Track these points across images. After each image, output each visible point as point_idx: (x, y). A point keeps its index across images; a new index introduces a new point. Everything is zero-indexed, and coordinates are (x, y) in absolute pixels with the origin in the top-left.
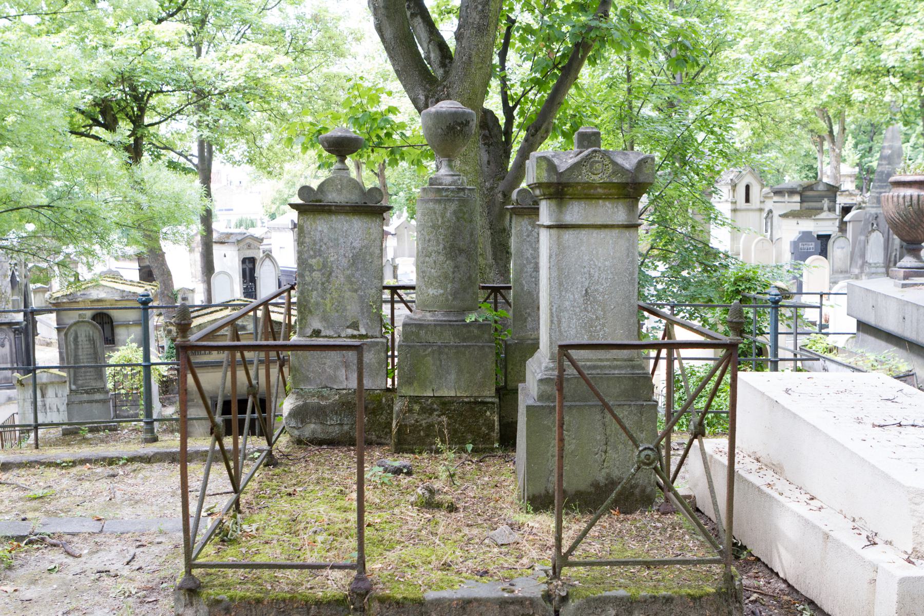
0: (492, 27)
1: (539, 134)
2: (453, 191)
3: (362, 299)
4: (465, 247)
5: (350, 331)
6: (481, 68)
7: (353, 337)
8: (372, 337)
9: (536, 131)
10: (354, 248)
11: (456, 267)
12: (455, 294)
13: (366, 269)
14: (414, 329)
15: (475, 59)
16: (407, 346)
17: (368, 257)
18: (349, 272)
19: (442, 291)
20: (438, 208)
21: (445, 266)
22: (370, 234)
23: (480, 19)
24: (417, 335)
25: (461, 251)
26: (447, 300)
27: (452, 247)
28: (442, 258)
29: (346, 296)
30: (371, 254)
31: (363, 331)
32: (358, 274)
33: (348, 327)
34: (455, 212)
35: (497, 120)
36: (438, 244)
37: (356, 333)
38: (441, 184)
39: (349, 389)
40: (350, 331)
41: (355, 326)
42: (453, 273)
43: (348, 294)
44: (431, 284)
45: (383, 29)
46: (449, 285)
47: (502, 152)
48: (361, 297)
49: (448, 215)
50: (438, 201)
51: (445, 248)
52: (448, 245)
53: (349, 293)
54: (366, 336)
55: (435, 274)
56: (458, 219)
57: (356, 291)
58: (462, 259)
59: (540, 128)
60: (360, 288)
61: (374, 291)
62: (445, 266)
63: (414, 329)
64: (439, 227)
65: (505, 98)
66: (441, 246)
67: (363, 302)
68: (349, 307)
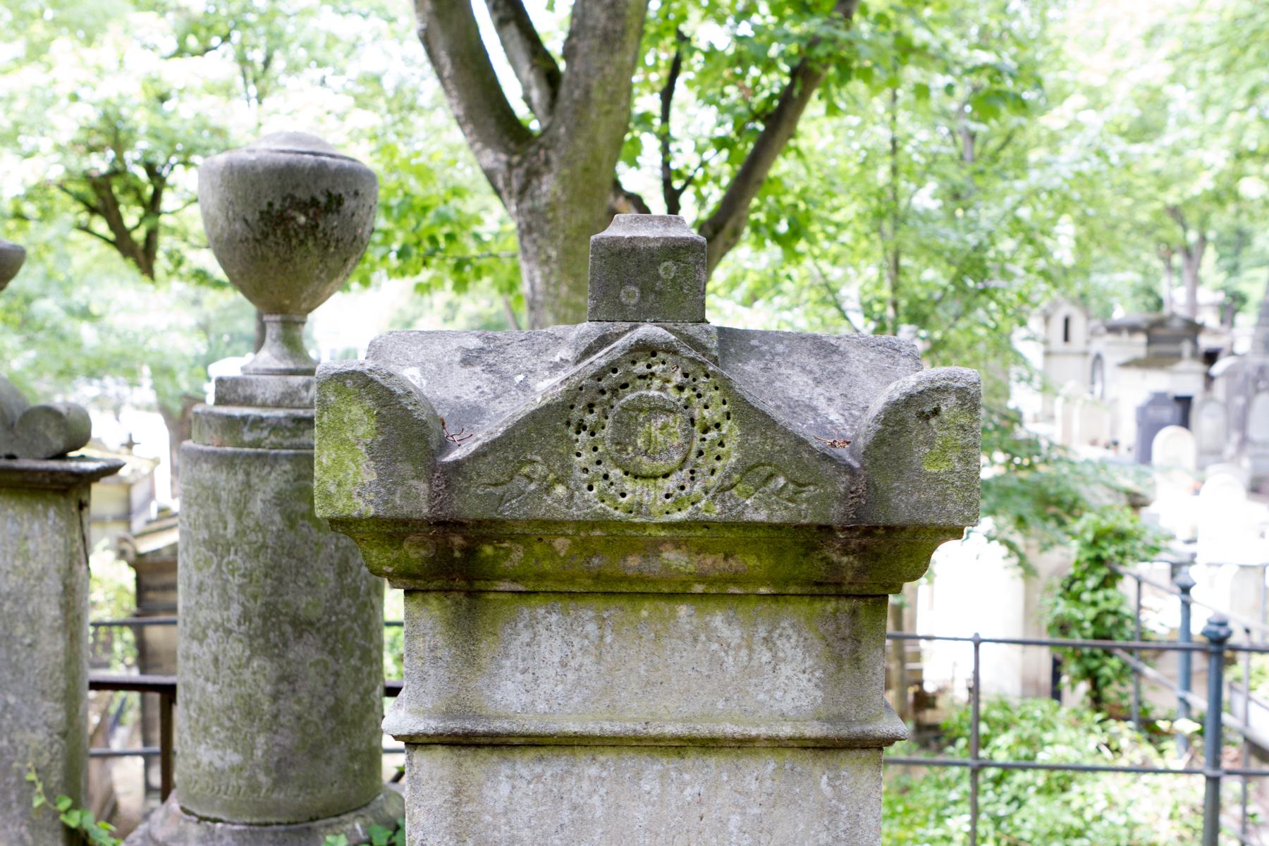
2: (276, 427)
4: (314, 614)
11: (283, 678)
12: (280, 769)
17: (20, 629)
19: (234, 758)
20: (227, 482)
21: (247, 675)
22: (27, 557)
25: (302, 626)
26: (254, 787)
27: (270, 613)
28: (237, 649)
30: (31, 621)
34: (280, 500)
36: (226, 601)
38: (248, 401)
42: (275, 697)
44: (206, 729)
46: (261, 740)
49: (257, 506)
50: (227, 461)
51: (246, 617)
52: (256, 607)
55: (217, 701)
56: (291, 521)
58: (306, 652)
61: (40, 735)
62: (247, 675)
64: (228, 546)
66: (236, 610)
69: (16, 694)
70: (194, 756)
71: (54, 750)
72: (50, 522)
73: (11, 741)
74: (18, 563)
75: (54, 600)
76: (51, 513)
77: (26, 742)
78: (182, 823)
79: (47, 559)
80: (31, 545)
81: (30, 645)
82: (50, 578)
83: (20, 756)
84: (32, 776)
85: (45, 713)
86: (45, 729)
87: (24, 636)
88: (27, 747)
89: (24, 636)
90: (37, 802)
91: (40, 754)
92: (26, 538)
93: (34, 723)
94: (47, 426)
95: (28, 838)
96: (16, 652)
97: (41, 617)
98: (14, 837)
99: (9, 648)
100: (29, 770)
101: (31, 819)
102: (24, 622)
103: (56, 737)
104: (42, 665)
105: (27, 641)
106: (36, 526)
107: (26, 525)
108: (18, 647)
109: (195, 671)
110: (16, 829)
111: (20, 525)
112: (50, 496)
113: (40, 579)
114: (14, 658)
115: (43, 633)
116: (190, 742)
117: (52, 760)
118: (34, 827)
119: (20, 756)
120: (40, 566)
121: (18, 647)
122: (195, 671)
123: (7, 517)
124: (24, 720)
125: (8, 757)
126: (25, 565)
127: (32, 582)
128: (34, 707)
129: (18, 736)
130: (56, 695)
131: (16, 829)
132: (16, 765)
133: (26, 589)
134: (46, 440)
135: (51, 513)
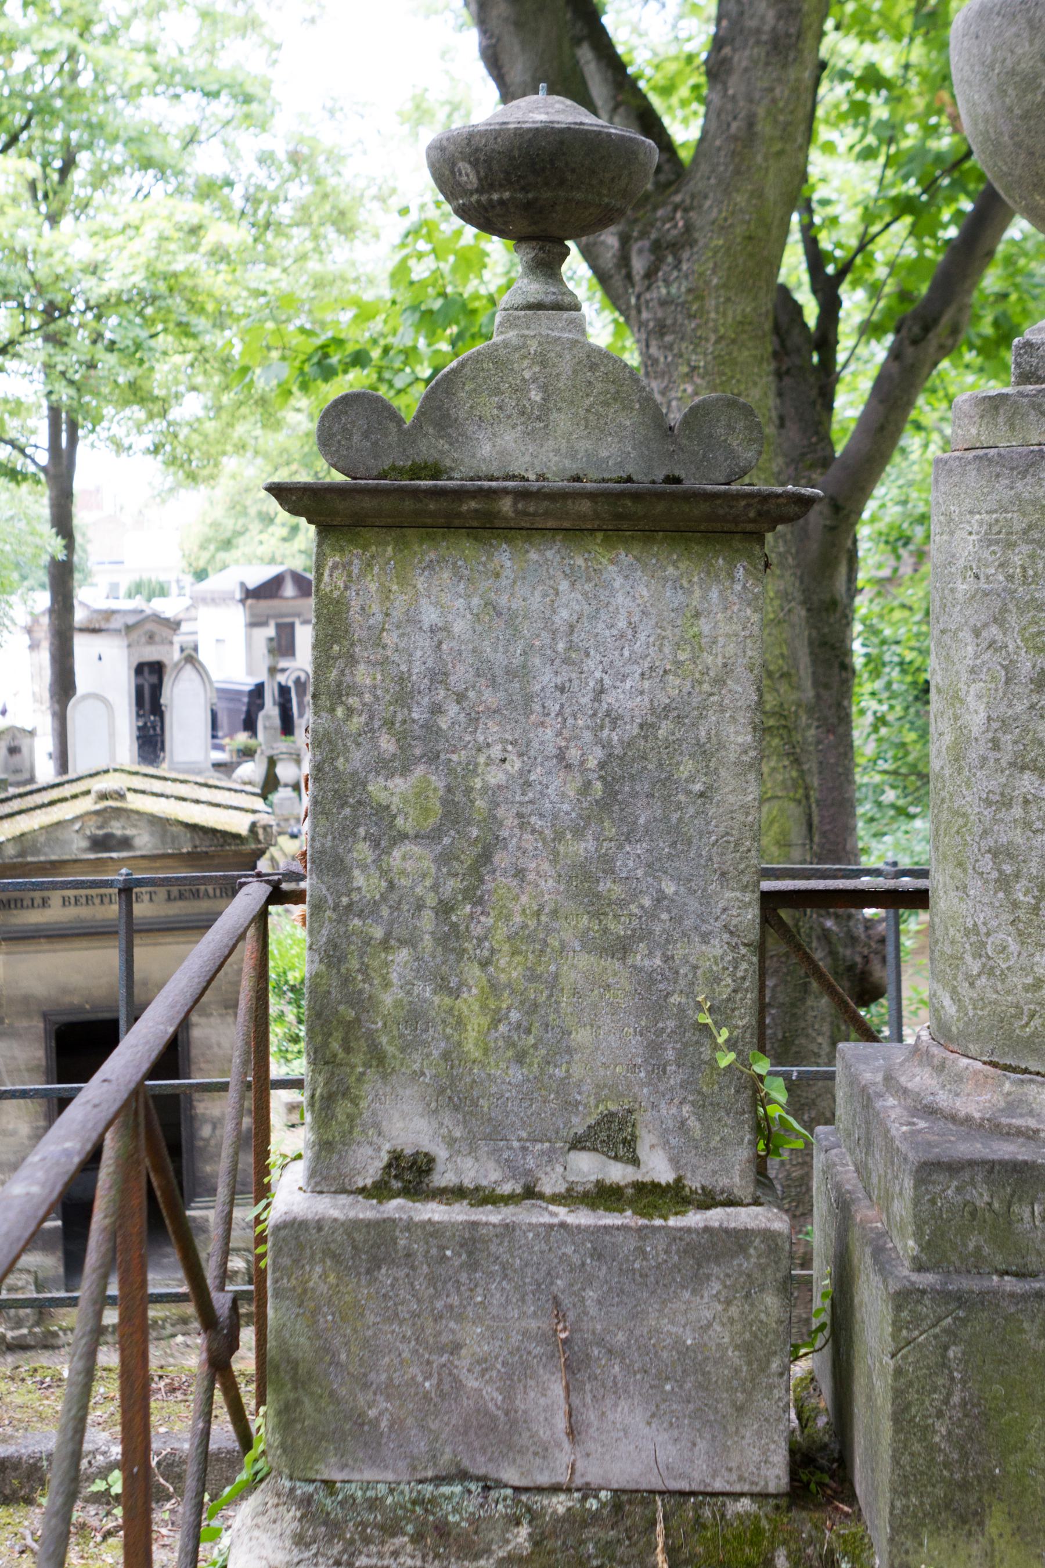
0: (810, 35)
1: (934, 339)
3: (652, 996)
5: (588, 1167)
6: (780, 153)
7: (605, 1196)
8: (708, 1200)
9: (927, 329)
10: (614, 719)
13: (677, 835)
14: (981, 1195)
15: (764, 128)
16: (943, 1296)
17: (686, 768)
18: (585, 847)
22: (697, 645)
23: (779, 17)
24: (1002, 1229)
29: (570, 977)
30: (704, 752)
31: (658, 1169)
32: (630, 859)
33: (577, 1144)
35: (797, 310)
37: (618, 1173)
39: (588, 1491)
40: (588, 1167)
41: (615, 1136)
43: (578, 967)
45: (504, 58)
47: (814, 393)
48: (648, 980)
53: (584, 961)
54: (673, 1196)
57: (621, 948)
59: (936, 321)
60: (643, 935)
61: (717, 948)
63: (981, 1195)
65: (816, 258)
67: (658, 1008)
68: (582, 1036)
69: (677, 879)
70: (1027, 970)
71: (740, 974)
72: (738, 587)
73: (667, 959)
74: (682, 656)
75: (743, 717)
76: (740, 573)
77: (693, 960)
78: (1007, 1087)
79: (731, 649)
80: (704, 626)
81: (702, 795)
82: (737, 681)
83: (682, 983)
84: (705, 1019)
85: (725, 910)
86: (726, 936)
87: (691, 779)
88: (695, 968)
89: (691, 779)
90: (726, 1059)
91: (717, 980)
92: (697, 615)
93: (704, 928)
94: (731, 428)
95: (693, 1123)
96: (679, 807)
97: (721, 746)
98: (670, 1124)
99: (666, 799)
100: (699, 1007)
101: (700, 1092)
102: (692, 756)
103: (743, 950)
104: (722, 829)
105: (698, 787)
106: (714, 595)
107: (697, 593)
108: (682, 797)
109: (1027, 825)
110: (674, 1110)
111: (689, 592)
112: (737, 544)
113: (719, 682)
114: (675, 817)
115: (723, 773)
116: (1013, 947)
117: (735, 991)
118: (704, 1105)
119: (682, 983)
120: (720, 661)
121: (682, 797)
122: (1027, 825)
123: (666, 579)
124: (688, 923)
125: (661, 986)
126: (694, 660)
127: (706, 687)
128: (706, 899)
129: (679, 951)
130: (745, 880)
131: (674, 1110)
132: (675, 999)
133: (695, 701)
134: (731, 454)
135: (740, 573)
